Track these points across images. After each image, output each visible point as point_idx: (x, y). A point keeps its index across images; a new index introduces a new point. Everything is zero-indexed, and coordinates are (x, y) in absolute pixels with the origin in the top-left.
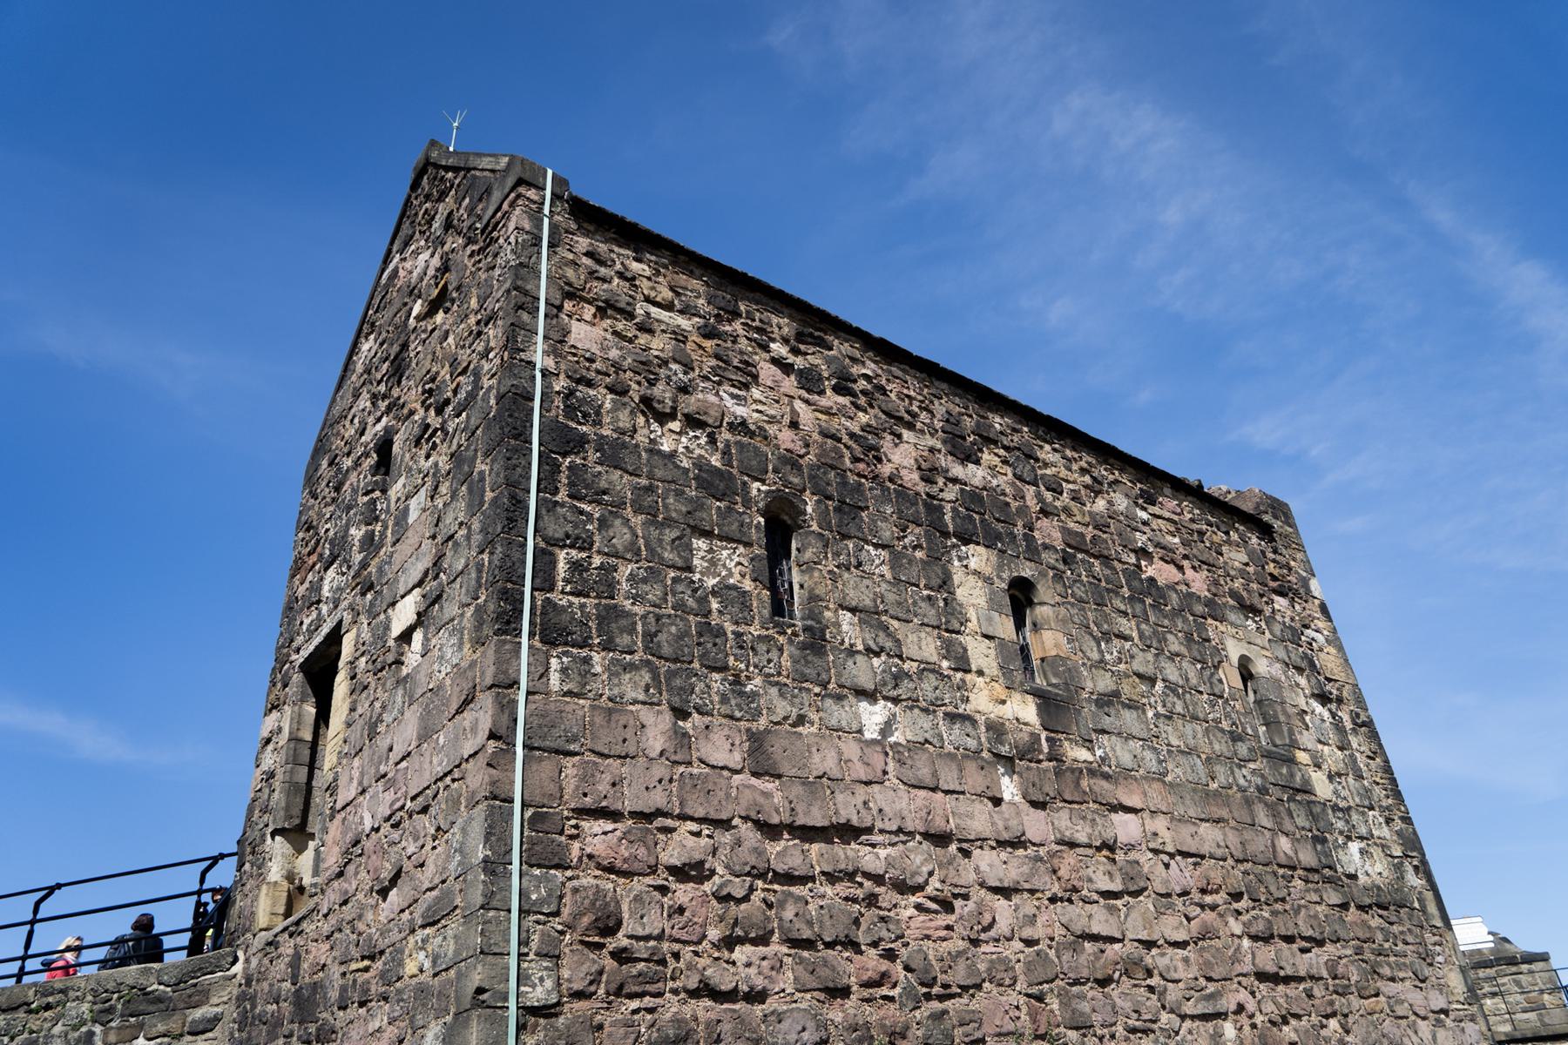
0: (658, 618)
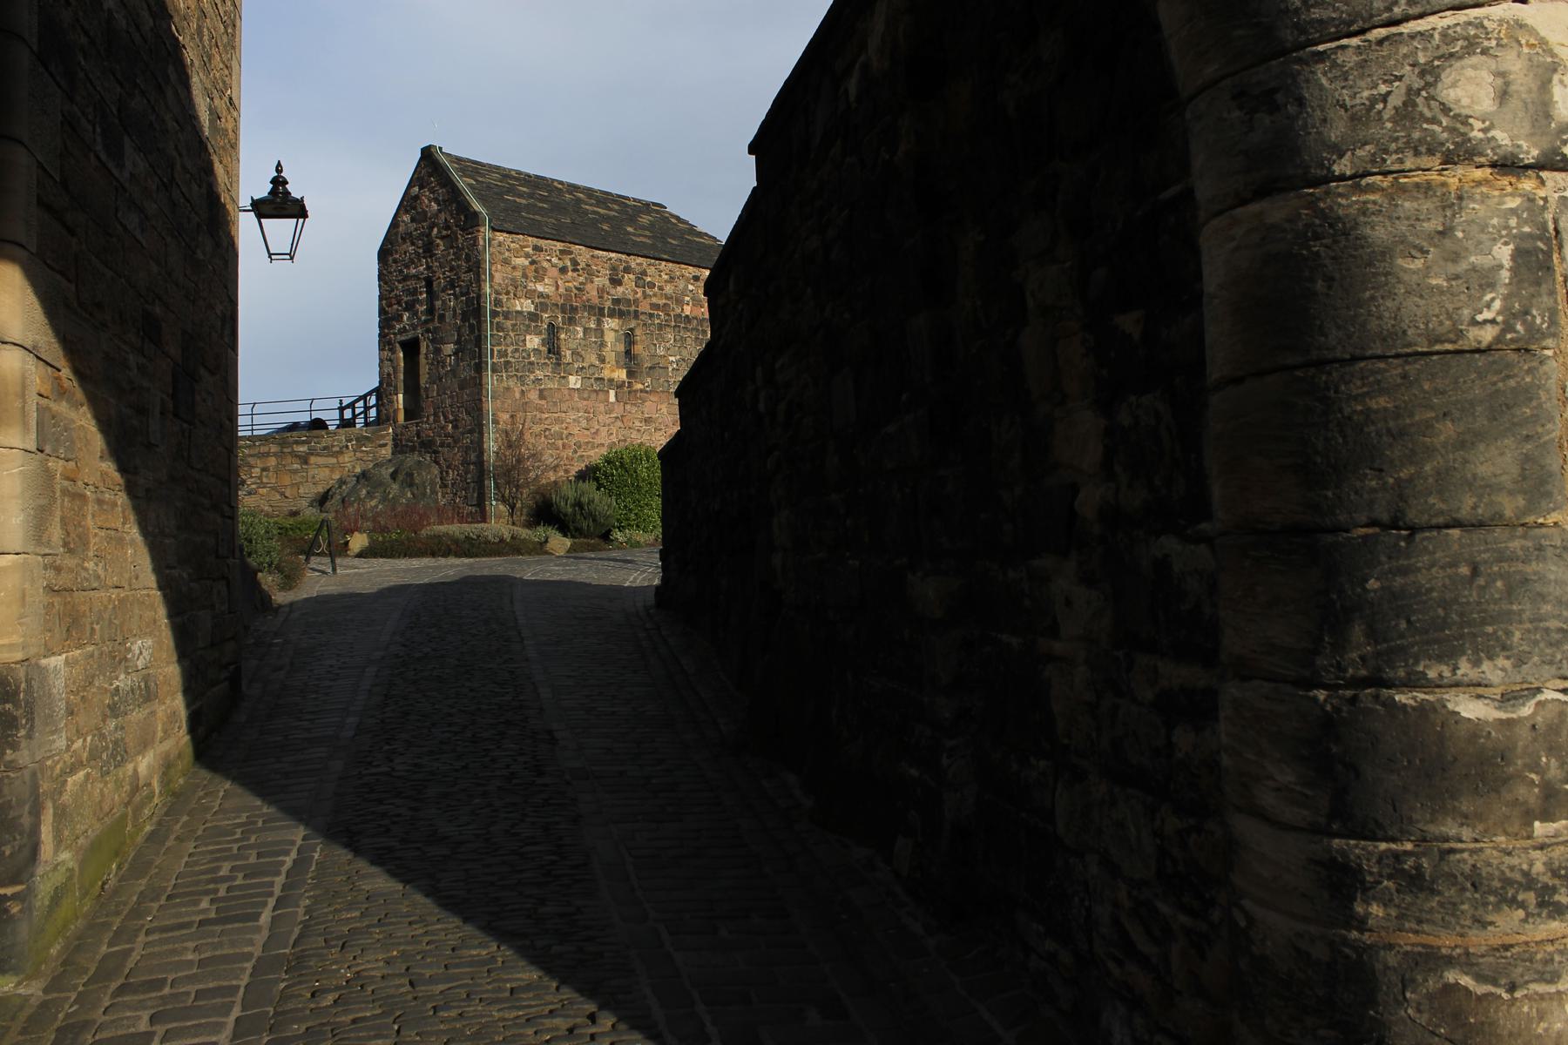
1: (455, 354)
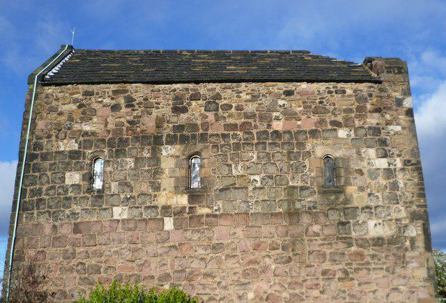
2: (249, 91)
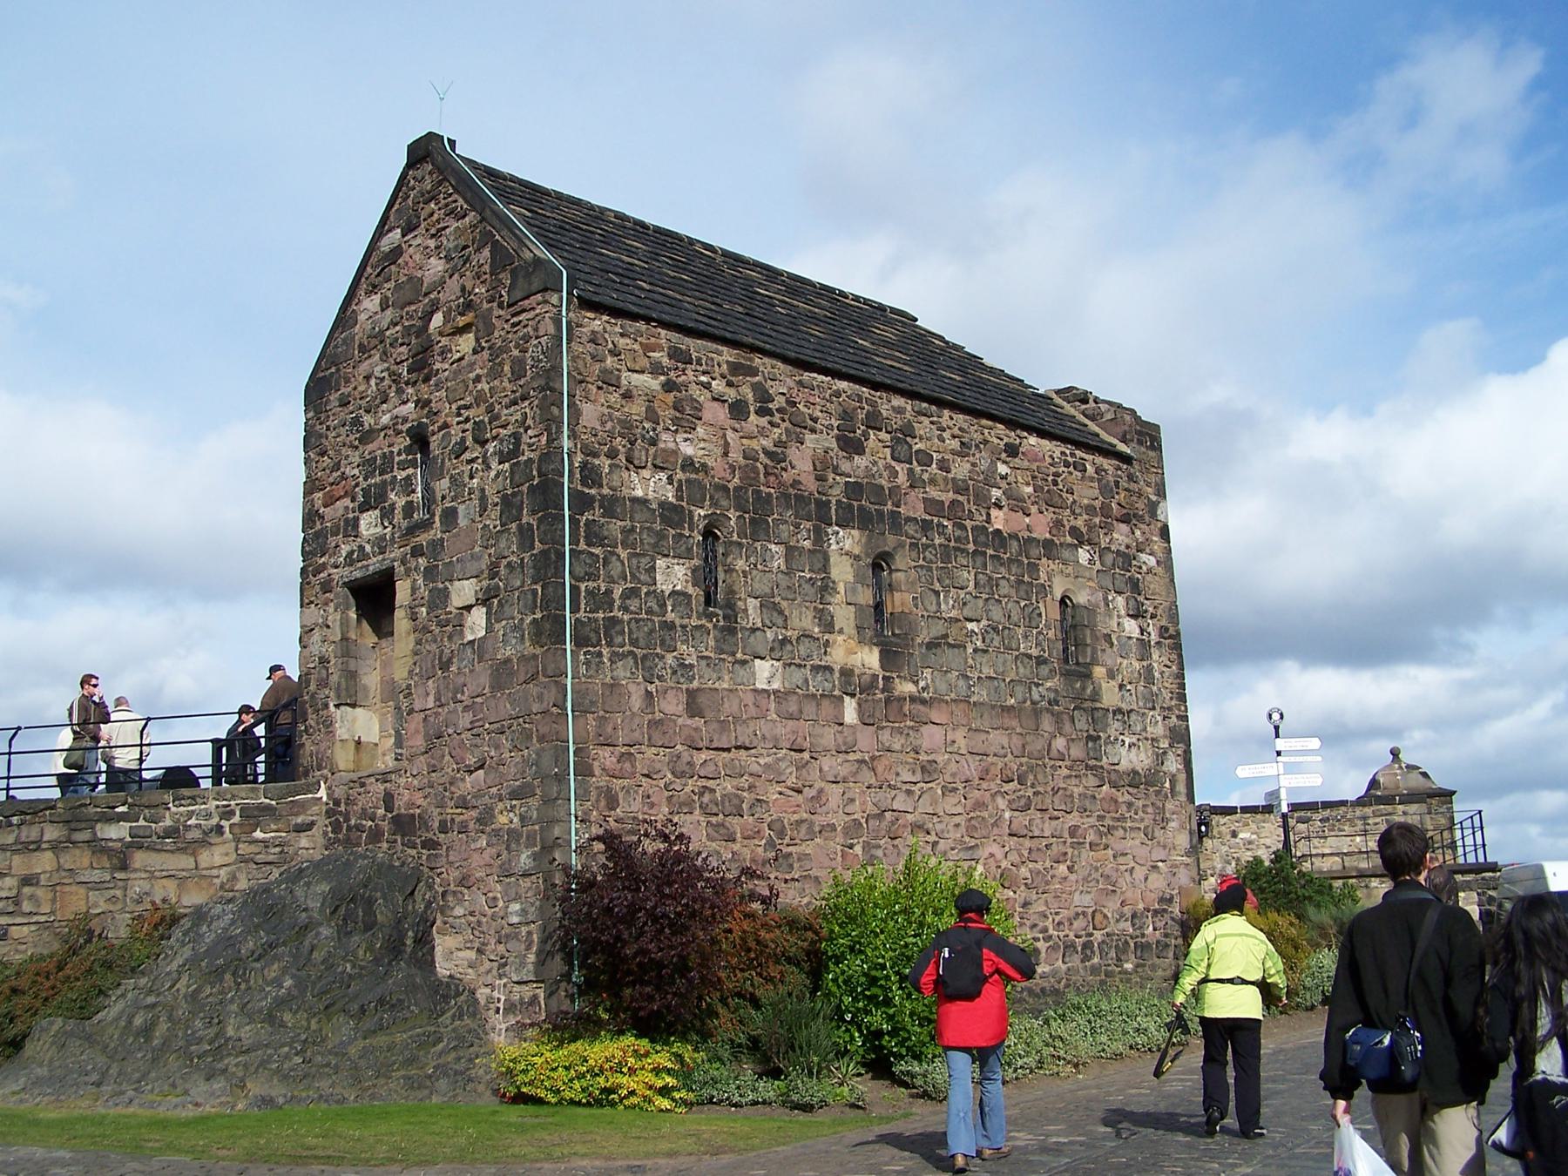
0: (637, 621)
1: (484, 601)
2: (956, 431)
